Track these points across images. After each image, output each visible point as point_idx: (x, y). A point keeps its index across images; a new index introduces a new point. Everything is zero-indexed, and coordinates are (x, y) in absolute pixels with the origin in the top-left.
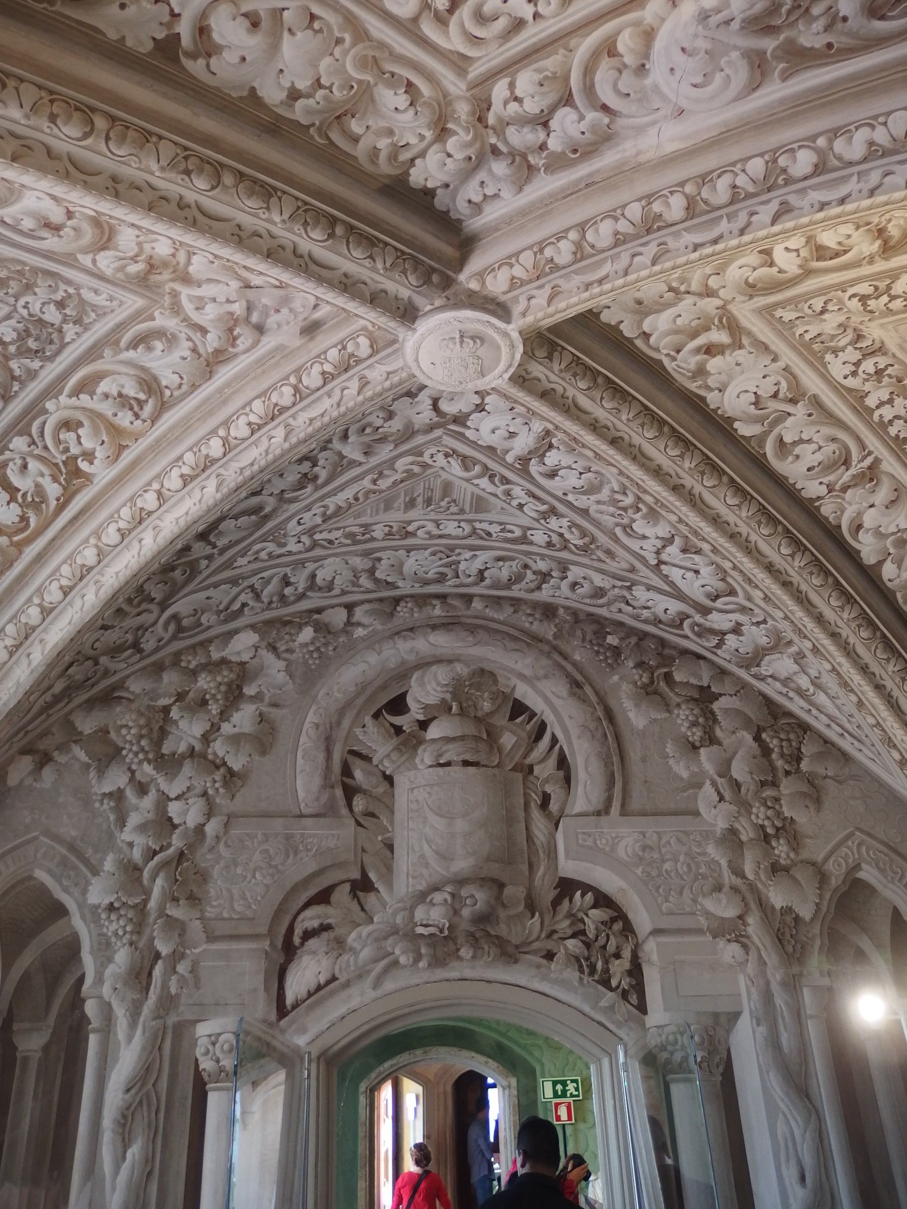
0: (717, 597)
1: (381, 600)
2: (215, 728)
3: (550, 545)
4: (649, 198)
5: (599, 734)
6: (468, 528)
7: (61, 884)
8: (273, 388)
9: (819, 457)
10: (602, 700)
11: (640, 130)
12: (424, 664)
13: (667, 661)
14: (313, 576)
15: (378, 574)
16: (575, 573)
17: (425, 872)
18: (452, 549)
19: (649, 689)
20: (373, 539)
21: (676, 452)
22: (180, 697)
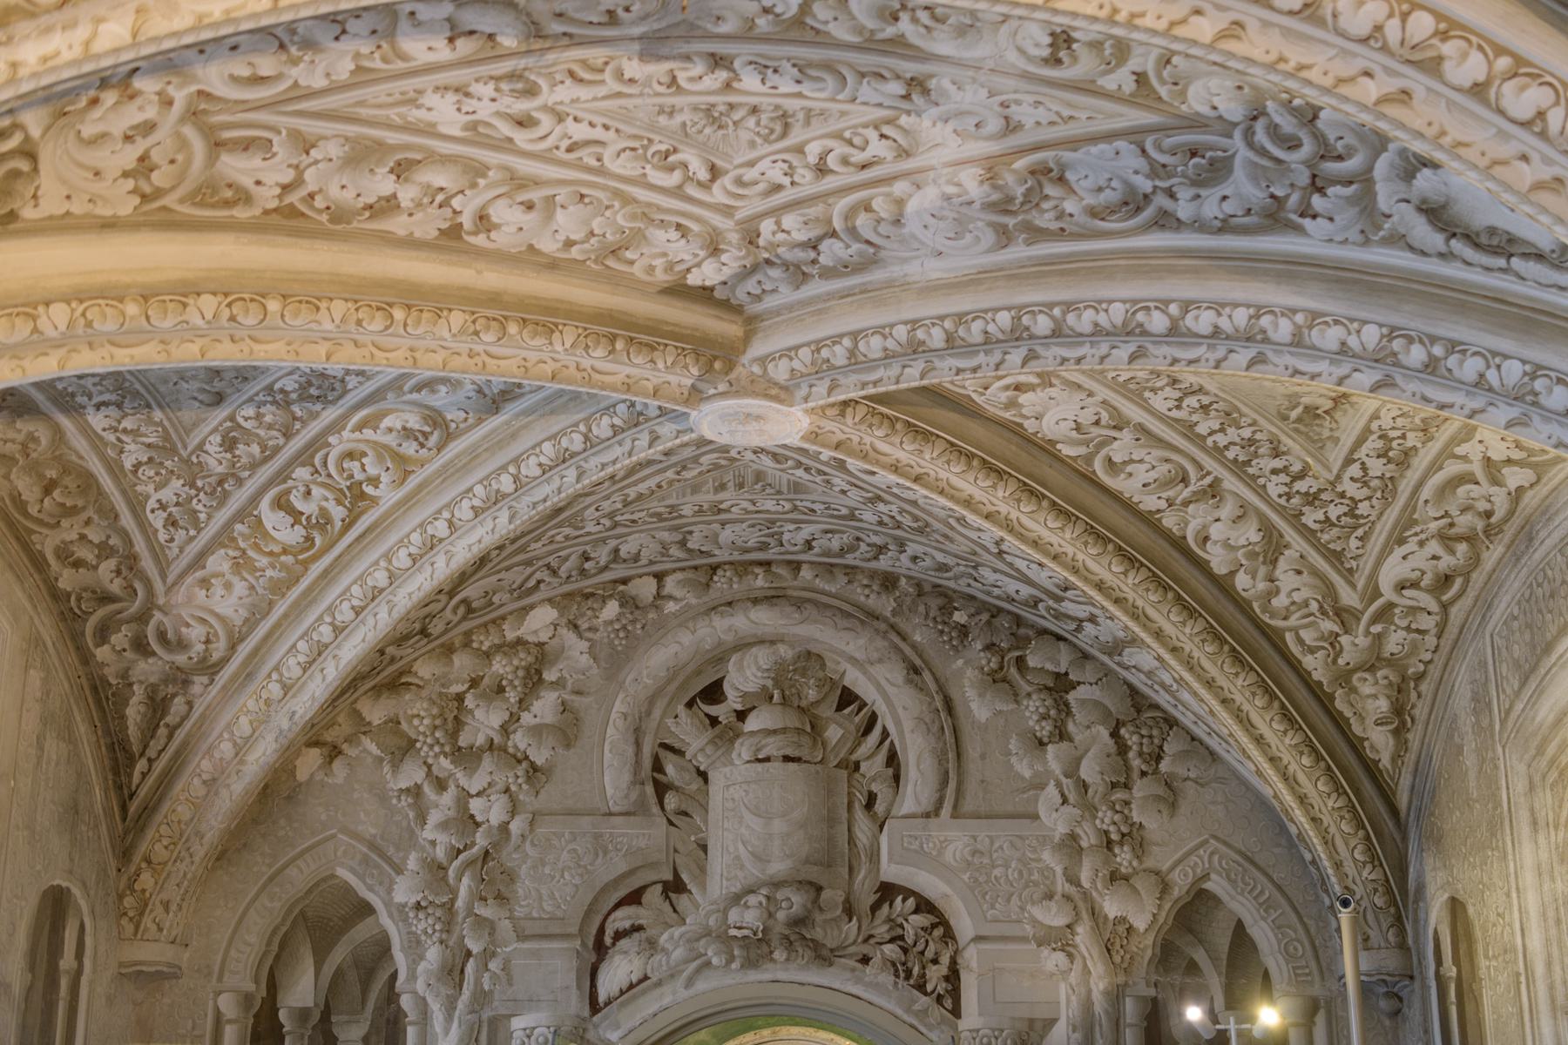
0: (1066, 589)
1: (696, 568)
2: (514, 718)
3: (881, 523)
4: (914, 323)
5: (935, 728)
6: (788, 506)
7: (364, 883)
8: (563, 432)
9: (1153, 475)
10: (941, 689)
11: (905, 261)
12: (742, 646)
13: (1021, 642)
14: (616, 551)
15: (690, 545)
16: (912, 548)
17: (740, 874)
18: (773, 522)
19: (998, 676)
20: (681, 516)
21: (988, 483)
22: (474, 683)
